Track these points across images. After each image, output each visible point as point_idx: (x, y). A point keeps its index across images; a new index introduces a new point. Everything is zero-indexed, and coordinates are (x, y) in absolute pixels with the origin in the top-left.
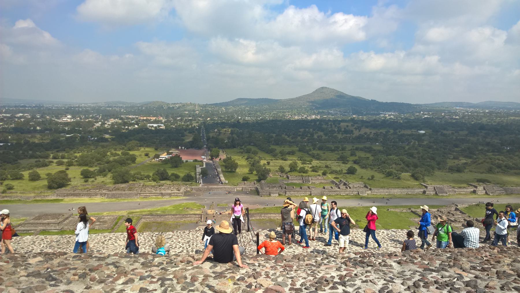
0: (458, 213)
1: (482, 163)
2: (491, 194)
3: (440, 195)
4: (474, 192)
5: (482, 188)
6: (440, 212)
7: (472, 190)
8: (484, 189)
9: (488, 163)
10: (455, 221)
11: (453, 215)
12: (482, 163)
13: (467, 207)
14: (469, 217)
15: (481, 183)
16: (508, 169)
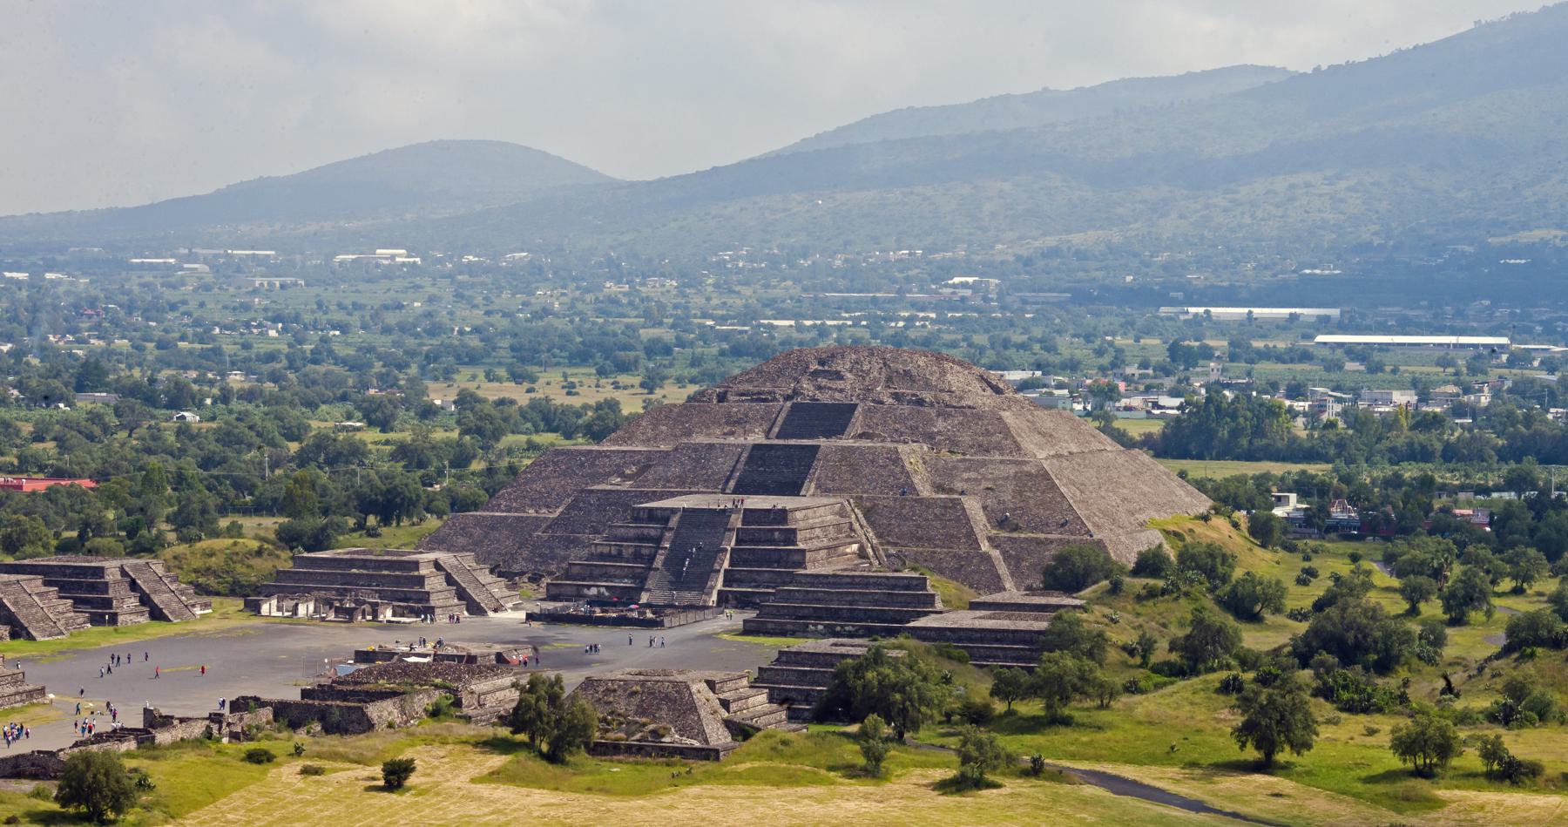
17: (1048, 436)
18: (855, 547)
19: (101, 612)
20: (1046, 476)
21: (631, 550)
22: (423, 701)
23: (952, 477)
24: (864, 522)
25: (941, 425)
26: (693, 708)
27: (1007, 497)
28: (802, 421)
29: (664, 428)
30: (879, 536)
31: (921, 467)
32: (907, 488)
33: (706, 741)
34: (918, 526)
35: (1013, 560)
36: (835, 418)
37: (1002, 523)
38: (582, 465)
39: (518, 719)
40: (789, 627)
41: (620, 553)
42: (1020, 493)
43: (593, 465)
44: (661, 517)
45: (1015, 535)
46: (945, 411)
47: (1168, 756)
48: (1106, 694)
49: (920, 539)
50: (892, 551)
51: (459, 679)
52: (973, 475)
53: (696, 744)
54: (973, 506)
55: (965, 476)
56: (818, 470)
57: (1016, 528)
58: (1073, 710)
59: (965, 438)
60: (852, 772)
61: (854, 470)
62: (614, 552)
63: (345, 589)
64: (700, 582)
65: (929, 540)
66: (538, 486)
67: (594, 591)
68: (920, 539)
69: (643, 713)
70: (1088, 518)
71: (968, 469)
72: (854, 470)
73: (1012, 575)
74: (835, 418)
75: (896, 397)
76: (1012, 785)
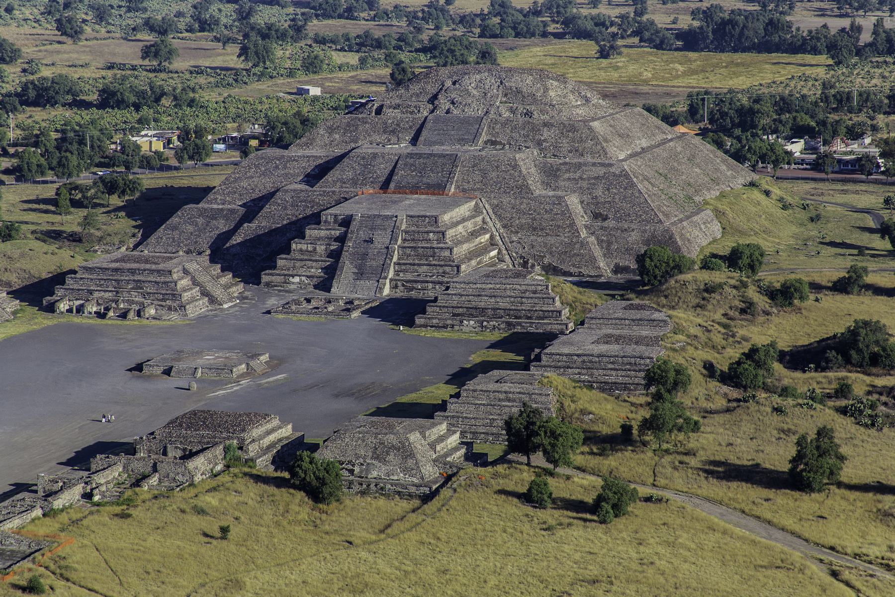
17: (625, 136)
18: (487, 236)
20: (627, 176)
21: (323, 247)
23: (556, 177)
24: (493, 217)
25: (546, 134)
26: (412, 455)
27: (599, 192)
29: (337, 136)
30: (504, 227)
31: (533, 170)
32: (523, 189)
33: (422, 478)
34: (534, 219)
35: (607, 246)
37: (596, 216)
38: (277, 167)
40: (449, 322)
41: (315, 249)
42: (608, 190)
43: (285, 167)
45: (606, 224)
49: (535, 229)
50: (515, 239)
51: (243, 430)
52: (572, 175)
53: (415, 480)
54: (573, 201)
55: (567, 176)
57: (605, 218)
59: (565, 144)
61: (484, 174)
62: (310, 248)
65: (542, 229)
66: (244, 184)
67: (297, 279)
68: (535, 229)
69: (377, 458)
70: (659, 209)
71: (568, 171)
72: (484, 174)
73: (605, 255)
75: (513, 111)
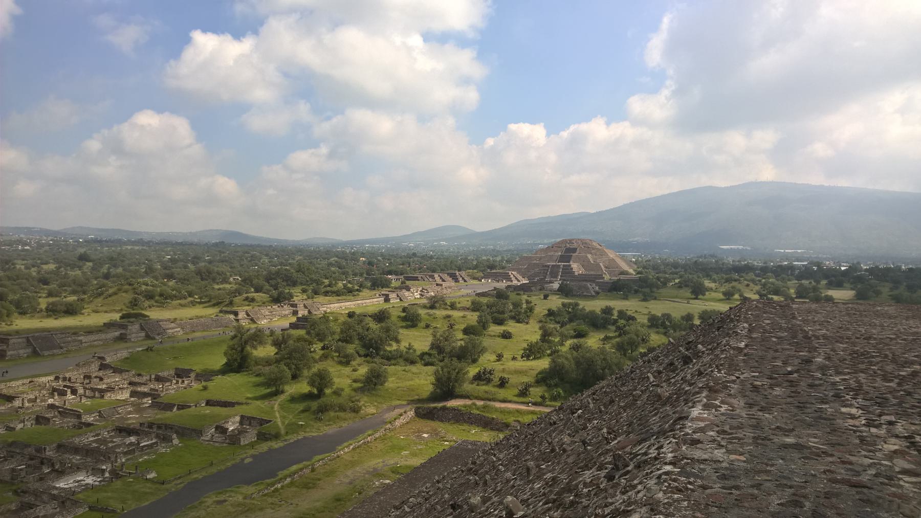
0: (109, 372)
1: (115, 294)
2: (157, 337)
3: (46, 353)
4: (122, 338)
5: (137, 326)
6: (65, 379)
7: (117, 334)
8: (142, 329)
9: (126, 292)
10: (110, 389)
11: (101, 379)
12: (115, 294)
13: (127, 358)
14: (139, 375)
15: (132, 320)
16: (166, 298)
19: (457, 281)
22: (539, 287)
28: (568, 251)
36: (574, 250)
39: (558, 290)
44: (548, 266)
46: (593, 249)
47: (676, 297)
48: (658, 288)
56: (573, 258)
58: (655, 290)
60: (624, 299)
63: (497, 277)
64: (556, 277)
74: (574, 250)
76: (652, 302)
